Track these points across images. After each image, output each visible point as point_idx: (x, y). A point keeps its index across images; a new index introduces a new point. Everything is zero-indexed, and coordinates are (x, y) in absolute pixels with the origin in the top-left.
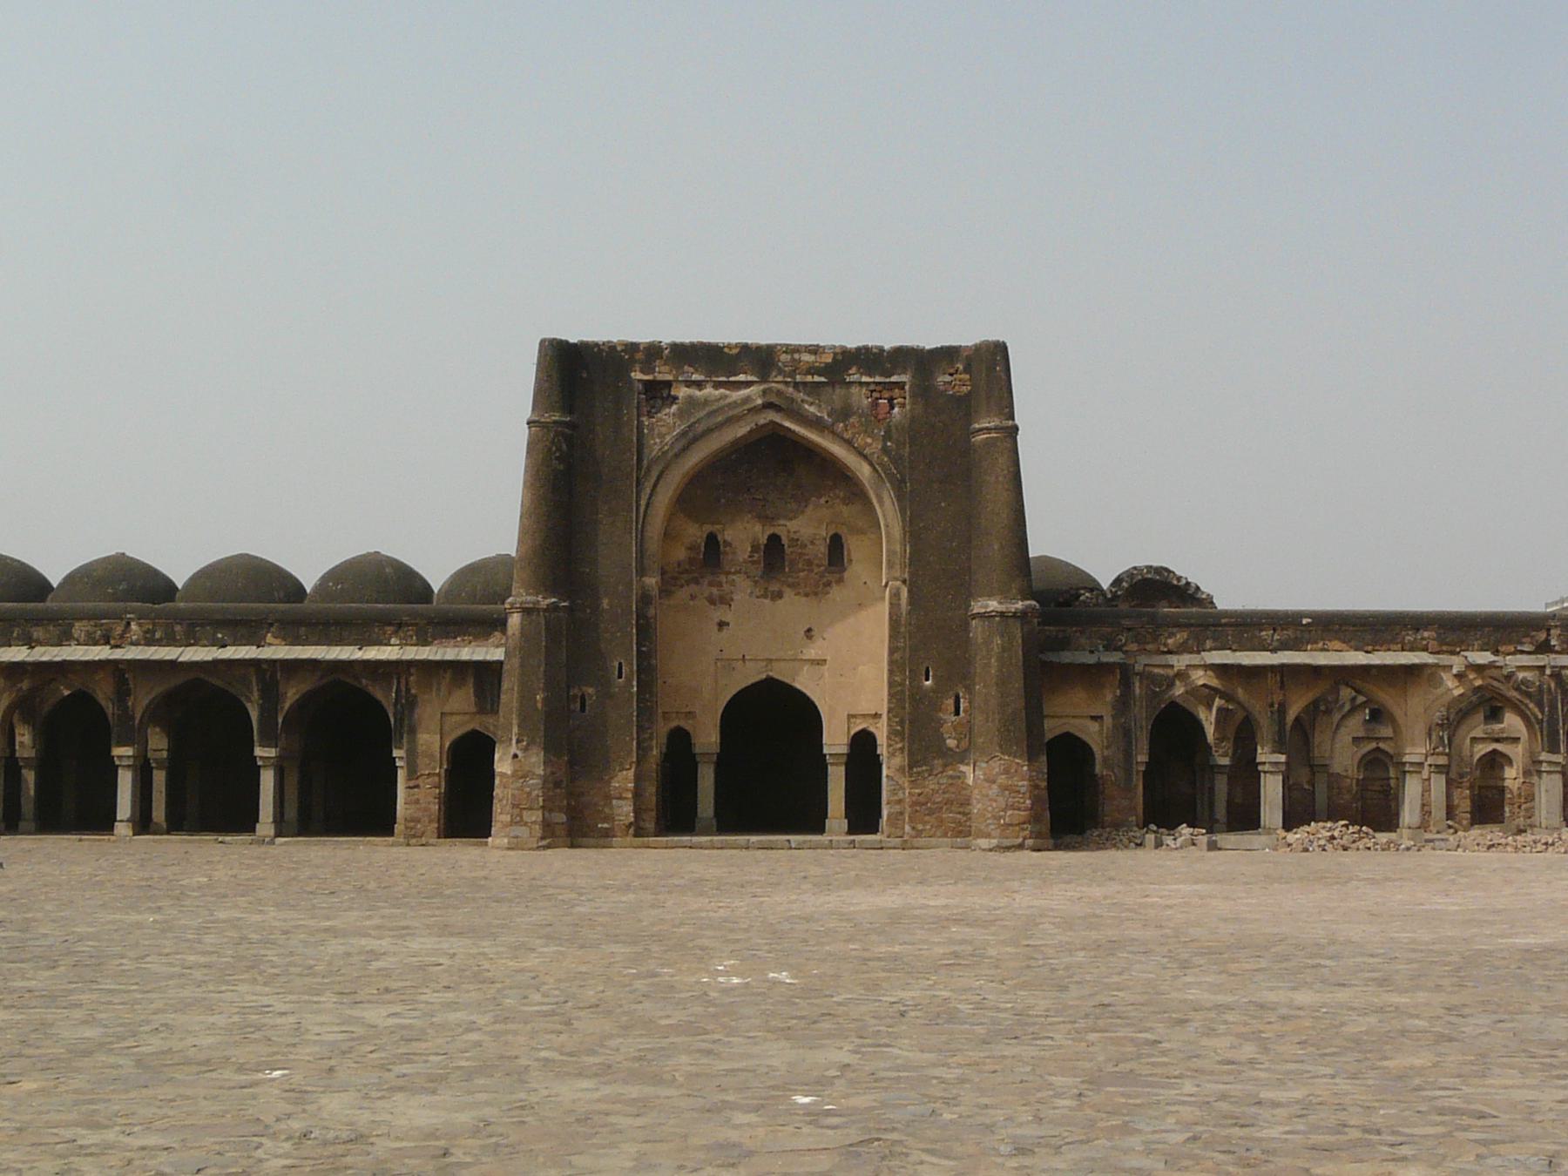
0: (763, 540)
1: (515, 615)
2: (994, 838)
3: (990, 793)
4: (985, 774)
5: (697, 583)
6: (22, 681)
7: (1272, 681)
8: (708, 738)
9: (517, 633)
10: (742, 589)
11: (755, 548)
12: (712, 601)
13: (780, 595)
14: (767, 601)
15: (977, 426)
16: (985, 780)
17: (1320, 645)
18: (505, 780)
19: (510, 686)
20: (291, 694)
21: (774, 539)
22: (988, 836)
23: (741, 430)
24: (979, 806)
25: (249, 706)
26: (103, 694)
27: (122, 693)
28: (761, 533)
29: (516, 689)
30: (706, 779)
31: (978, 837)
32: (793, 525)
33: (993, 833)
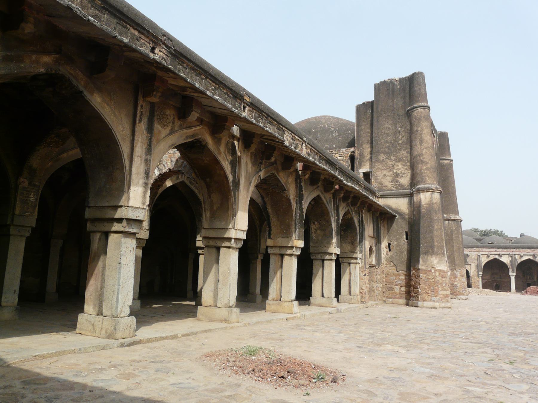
1: (436, 193)
2: (465, 295)
3: (462, 280)
4: (460, 273)
6: (260, 170)
9: (438, 202)
15: (443, 157)
16: (460, 276)
18: (442, 274)
19: (439, 227)
22: (463, 294)
24: (459, 284)
25: (332, 218)
29: (443, 229)
31: (460, 295)
33: (465, 294)
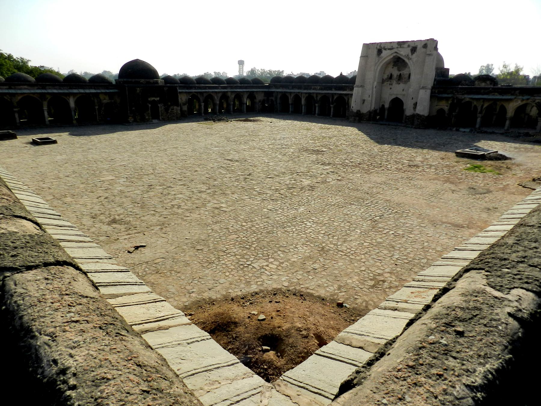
0: (399, 74)
5: (388, 81)
7: (481, 101)
8: (387, 106)
10: (394, 82)
11: (397, 76)
12: (390, 84)
13: (399, 84)
14: (397, 85)
17: (493, 94)
20: (335, 97)
21: (400, 74)
23: (392, 57)
26: (315, 96)
27: (317, 97)
28: (399, 73)
30: (386, 112)
32: (403, 72)
